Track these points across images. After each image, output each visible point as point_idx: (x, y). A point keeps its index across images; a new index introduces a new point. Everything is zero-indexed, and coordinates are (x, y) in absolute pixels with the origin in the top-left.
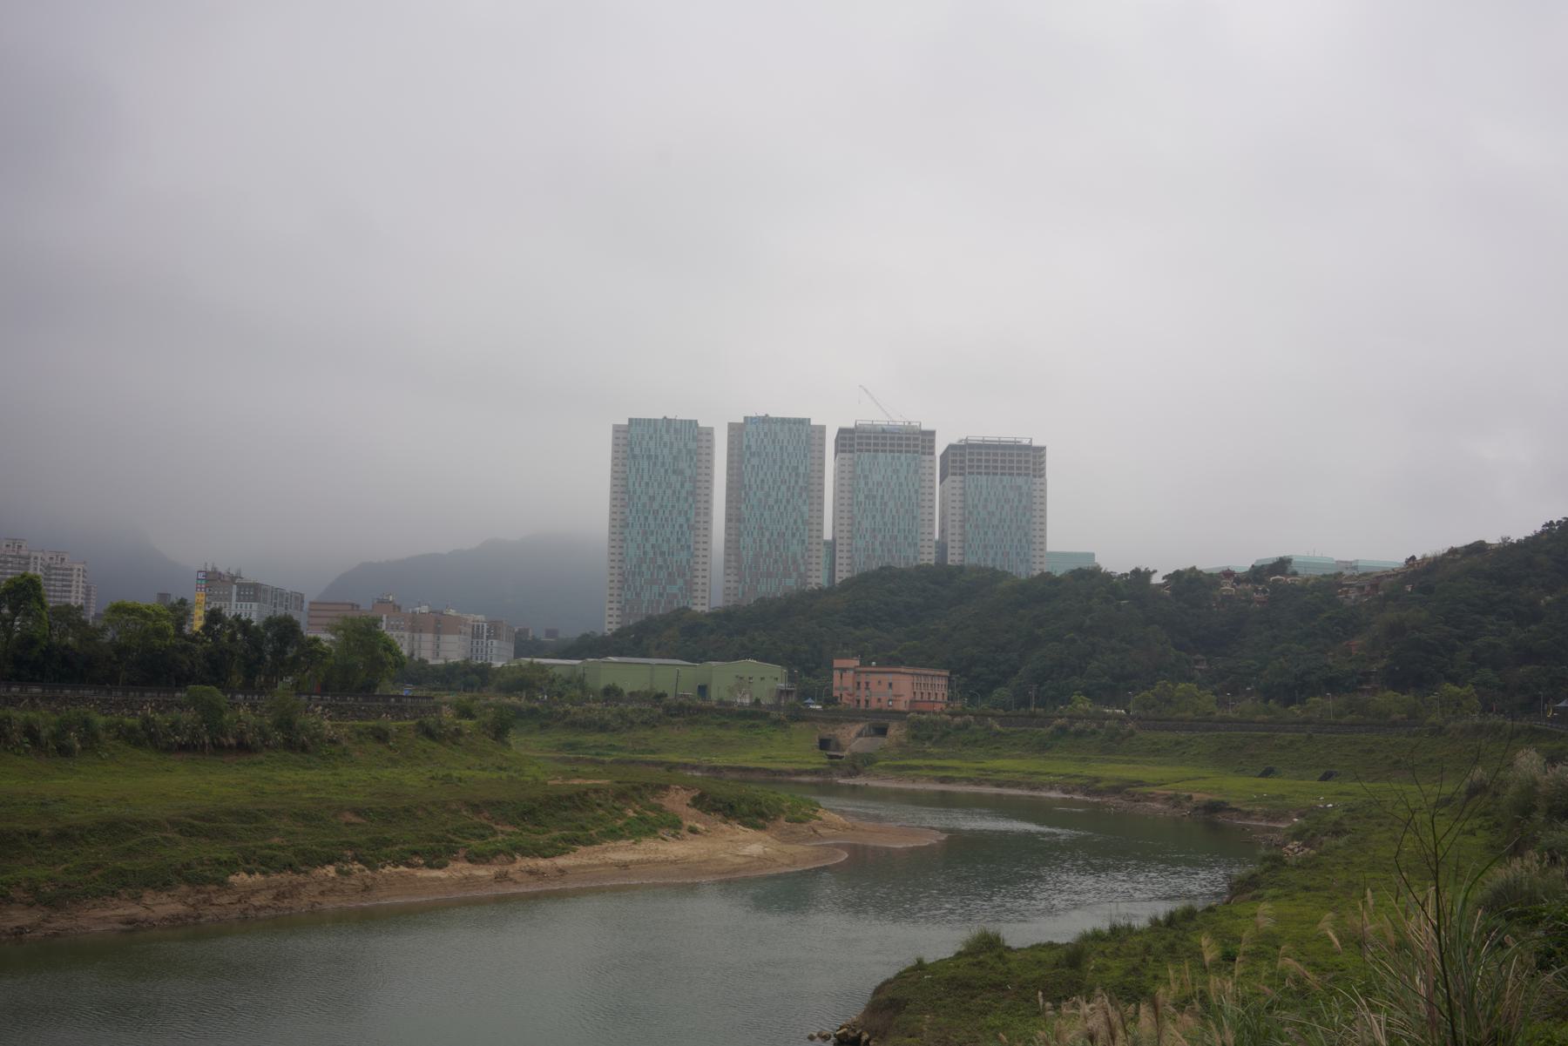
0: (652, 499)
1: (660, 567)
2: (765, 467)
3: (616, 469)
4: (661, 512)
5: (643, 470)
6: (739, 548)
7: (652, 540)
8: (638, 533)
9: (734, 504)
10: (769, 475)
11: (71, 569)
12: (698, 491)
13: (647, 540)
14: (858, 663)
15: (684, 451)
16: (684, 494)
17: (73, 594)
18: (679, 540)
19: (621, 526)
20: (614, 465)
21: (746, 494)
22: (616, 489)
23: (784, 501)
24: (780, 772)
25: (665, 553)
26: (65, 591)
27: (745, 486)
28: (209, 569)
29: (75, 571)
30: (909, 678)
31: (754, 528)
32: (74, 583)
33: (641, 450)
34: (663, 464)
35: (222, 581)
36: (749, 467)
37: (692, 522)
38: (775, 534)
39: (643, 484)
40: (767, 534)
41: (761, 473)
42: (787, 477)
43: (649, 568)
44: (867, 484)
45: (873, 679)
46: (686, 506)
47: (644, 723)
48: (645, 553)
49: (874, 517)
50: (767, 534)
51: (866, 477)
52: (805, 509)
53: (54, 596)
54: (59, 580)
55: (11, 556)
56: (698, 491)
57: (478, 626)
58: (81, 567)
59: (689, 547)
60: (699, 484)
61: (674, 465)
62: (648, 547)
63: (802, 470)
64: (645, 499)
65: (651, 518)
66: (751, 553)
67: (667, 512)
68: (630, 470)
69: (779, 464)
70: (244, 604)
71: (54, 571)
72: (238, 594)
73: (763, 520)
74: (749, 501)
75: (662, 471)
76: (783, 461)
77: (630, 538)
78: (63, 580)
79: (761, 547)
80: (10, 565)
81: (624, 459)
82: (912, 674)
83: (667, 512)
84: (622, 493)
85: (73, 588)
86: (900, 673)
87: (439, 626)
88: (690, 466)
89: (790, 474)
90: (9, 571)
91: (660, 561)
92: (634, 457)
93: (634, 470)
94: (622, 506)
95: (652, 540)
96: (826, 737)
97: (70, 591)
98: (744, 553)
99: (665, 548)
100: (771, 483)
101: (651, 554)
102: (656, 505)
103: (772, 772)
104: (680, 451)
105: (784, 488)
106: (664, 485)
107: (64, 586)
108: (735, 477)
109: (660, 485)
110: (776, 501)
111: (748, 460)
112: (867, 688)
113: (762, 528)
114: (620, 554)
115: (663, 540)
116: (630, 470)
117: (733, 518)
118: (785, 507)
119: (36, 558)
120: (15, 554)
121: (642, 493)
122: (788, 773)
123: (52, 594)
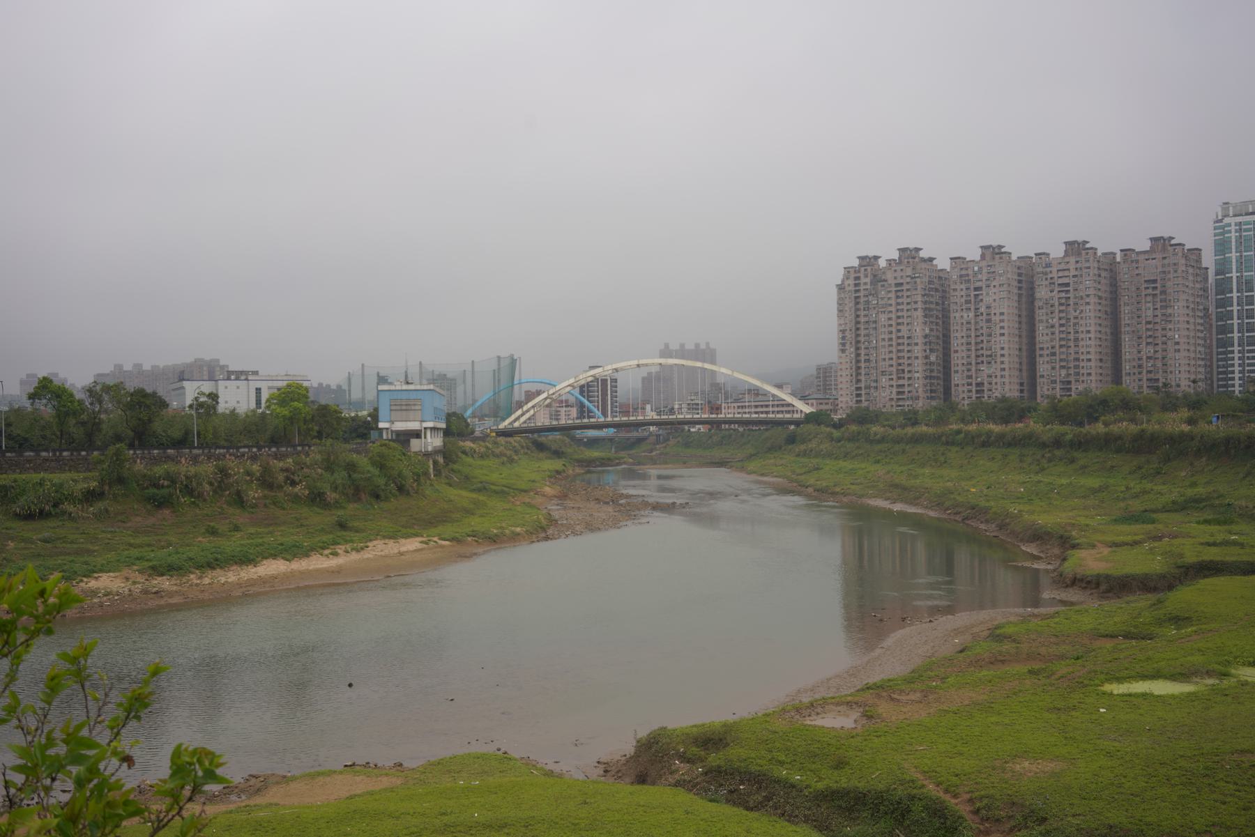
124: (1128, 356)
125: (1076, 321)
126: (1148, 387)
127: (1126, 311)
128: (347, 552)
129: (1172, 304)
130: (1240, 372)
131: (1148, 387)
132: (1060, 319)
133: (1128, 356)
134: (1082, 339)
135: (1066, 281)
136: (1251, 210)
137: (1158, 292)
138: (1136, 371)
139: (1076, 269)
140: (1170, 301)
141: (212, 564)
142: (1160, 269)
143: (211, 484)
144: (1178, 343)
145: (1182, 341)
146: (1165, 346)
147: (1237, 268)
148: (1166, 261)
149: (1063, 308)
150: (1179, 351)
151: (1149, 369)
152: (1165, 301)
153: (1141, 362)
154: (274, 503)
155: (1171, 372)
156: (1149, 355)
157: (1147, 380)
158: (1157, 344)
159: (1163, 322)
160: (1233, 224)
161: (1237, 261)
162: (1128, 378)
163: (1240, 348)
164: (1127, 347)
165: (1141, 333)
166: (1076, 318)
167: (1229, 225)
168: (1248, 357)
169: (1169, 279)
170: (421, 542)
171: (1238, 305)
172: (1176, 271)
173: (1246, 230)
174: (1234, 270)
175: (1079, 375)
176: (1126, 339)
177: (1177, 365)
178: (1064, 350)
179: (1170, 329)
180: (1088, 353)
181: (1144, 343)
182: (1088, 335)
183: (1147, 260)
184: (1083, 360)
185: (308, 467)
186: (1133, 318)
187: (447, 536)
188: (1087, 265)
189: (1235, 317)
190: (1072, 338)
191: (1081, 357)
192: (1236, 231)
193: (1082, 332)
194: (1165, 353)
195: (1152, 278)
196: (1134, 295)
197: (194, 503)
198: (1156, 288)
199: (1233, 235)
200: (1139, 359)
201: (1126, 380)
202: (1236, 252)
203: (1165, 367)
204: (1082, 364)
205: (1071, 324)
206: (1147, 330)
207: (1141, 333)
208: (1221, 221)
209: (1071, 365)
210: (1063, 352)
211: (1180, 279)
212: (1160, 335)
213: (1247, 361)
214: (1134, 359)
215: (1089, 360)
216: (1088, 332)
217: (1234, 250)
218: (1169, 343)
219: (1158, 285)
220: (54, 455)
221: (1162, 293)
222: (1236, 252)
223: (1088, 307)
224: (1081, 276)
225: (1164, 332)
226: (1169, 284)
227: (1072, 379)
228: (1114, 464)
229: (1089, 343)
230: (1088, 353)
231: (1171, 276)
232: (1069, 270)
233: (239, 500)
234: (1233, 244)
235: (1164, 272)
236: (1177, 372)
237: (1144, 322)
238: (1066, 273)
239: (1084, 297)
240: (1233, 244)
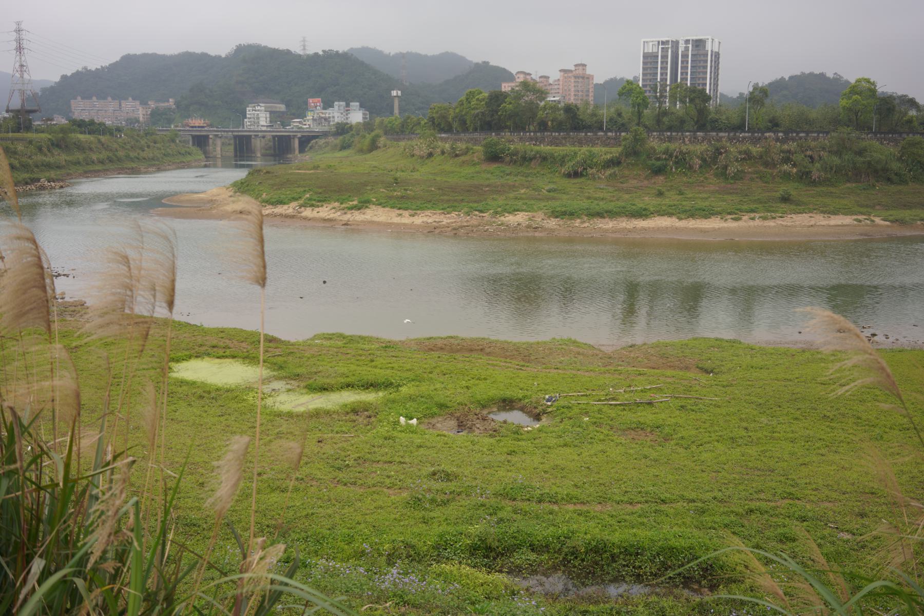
128: (753, 219)
141: (600, 215)
143: (704, 160)
154: (761, 178)
170: (855, 220)
185: (811, 149)
187: (891, 218)
197: (684, 173)
220: (616, 135)
233: (723, 174)
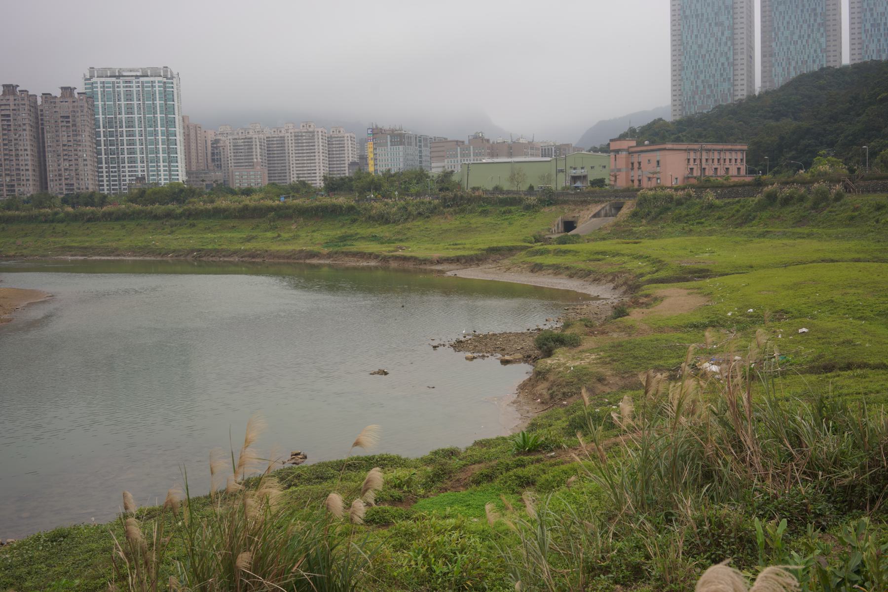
0: (700, 46)
1: (709, 96)
2: (790, 12)
3: (674, 28)
4: (707, 56)
5: (693, 26)
6: (771, 76)
7: (702, 77)
8: (691, 73)
9: (768, 43)
10: (793, 17)
11: (343, 137)
12: (736, 36)
13: (698, 78)
14: (634, 143)
15: (723, 7)
16: (724, 39)
17: (346, 152)
18: (722, 75)
19: (679, 70)
20: (673, 25)
21: (776, 34)
22: (675, 43)
23: (806, 36)
24: (425, 261)
25: (711, 85)
26: (342, 150)
27: (775, 28)
28: (374, 127)
29: (346, 138)
30: (683, 156)
31: (783, 60)
32: (346, 145)
33: (691, 11)
34: (707, 20)
35: (382, 133)
36: (777, 13)
37: (731, 60)
38: (800, 63)
39: (694, 37)
40: (793, 64)
41: (787, 18)
42: (807, 17)
43: (700, 98)
44: (872, 15)
45: (644, 158)
46: (726, 49)
47: (420, 214)
48: (697, 87)
49: (879, 40)
50: (793, 64)
51: (871, 10)
52: (823, 40)
53: (337, 154)
54: (337, 144)
55: (304, 132)
56: (736, 36)
57: (549, 149)
58: (348, 135)
59: (729, 79)
60: (736, 31)
61: (716, 20)
62: (699, 82)
63: (819, 10)
64: (695, 47)
65: (700, 61)
66: (781, 79)
67: (712, 55)
68: (684, 27)
69: (800, 7)
70: (395, 147)
71: (334, 139)
72: (391, 141)
73: (789, 53)
74: (778, 40)
75: (707, 25)
76: (803, 6)
77: (685, 77)
78: (339, 144)
79: (789, 73)
80: (304, 138)
81: (679, 20)
82: (685, 150)
83: (712, 55)
84: (679, 45)
85: (346, 148)
86: (665, 149)
87: (511, 151)
88: (728, 18)
89: (810, 15)
90: (304, 141)
91: (708, 92)
92: (686, 17)
93: (686, 27)
94: (679, 55)
95: (702, 77)
96: (570, 219)
97: (344, 150)
98: (776, 79)
99: (711, 81)
100: (795, 22)
101: (701, 88)
102: (703, 52)
103: (420, 260)
104: (720, 8)
105: (805, 26)
106: (709, 36)
107: (341, 147)
108: (767, 23)
109: (706, 37)
110: (800, 37)
111: (777, 8)
112: (639, 168)
113: (789, 59)
114: (680, 90)
115: (710, 77)
116: (684, 27)
117: (767, 54)
118: (807, 41)
119: (318, 132)
120: (306, 130)
121: (693, 42)
122: (432, 262)
123: (334, 152)
124: (51, 168)
125: (16, 142)
126: (66, 189)
127: (49, 137)
129: (80, 133)
130: (107, 181)
131: (66, 189)
132: (3, 140)
133: (51, 168)
134: (21, 155)
135: (7, 113)
136: (109, 74)
137: (70, 125)
138: (57, 178)
139: (15, 105)
140: (79, 131)
142: (71, 109)
144: (85, 160)
145: (88, 158)
146: (76, 162)
147: (102, 112)
148: (75, 104)
149: (6, 132)
150: (87, 165)
151: (66, 177)
152: (76, 131)
153: (60, 172)
155: (82, 179)
156: (66, 167)
157: (66, 184)
158: (71, 160)
159: (75, 146)
160: (99, 82)
161: (102, 107)
162: (52, 183)
163: (107, 165)
164: (50, 161)
165: (59, 152)
166: (16, 140)
167: (96, 83)
168: (112, 171)
169: (78, 117)
171: (104, 137)
172: (82, 111)
173: (108, 87)
174: (101, 113)
175: (20, 180)
176: (49, 156)
177: (86, 175)
178: (7, 162)
179: (80, 151)
180: (26, 165)
181: (62, 159)
182: (26, 152)
183: (61, 102)
184: (23, 170)
186: (53, 142)
188: (23, 102)
189: (103, 145)
190: (14, 154)
191: (22, 168)
192: (101, 88)
193: (21, 150)
194: (77, 166)
195: (66, 115)
196: (54, 126)
198: (69, 122)
199: (99, 90)
200: (59, 170)
201: (51, 185)
202: (102, 101)
203: (77, 176)
204: (22, 173)
205: (13, 144)
206: (64, 150)
207: (59, 152)
208: (89, 79)
209: (14, 173)
210: (7, 164)
211: (85, 117)
212: (73, 154)
213: (111, 174)
214: (55, 170)
215: (27, 170)
216: (26, 150)
217: (100, 100)
218: (80, 160)
219: (70, 120)
221: (73, 125)
222: (102, 101)
223: (25, 133)
224: (19, 110)
225: (76, 152)
226: (78, 120)
227: (15, 183)
228: (235, 225)
229: (26, 157)
230: (26, 165)
231: (79, 114)
232: (9, 105)
234: (100, 95)
235: (74, 111)
236: (86, 179)
237: (61, 145)
238: (7, 107)
239: (21, 125)
240: (100, 95)
